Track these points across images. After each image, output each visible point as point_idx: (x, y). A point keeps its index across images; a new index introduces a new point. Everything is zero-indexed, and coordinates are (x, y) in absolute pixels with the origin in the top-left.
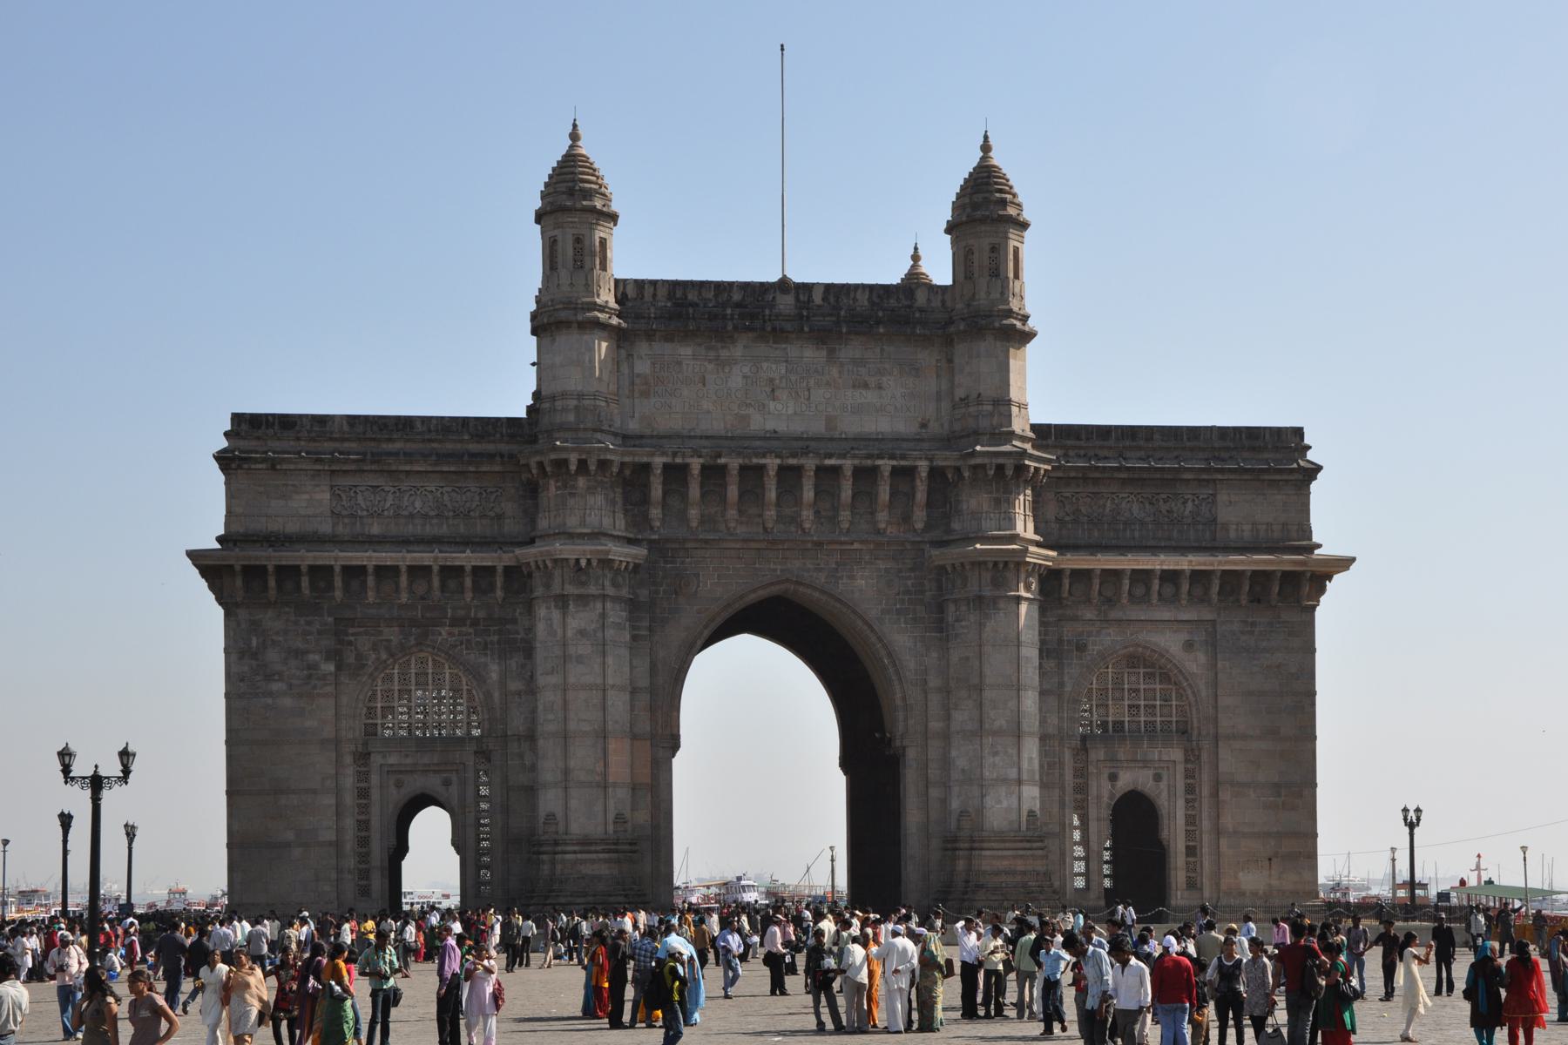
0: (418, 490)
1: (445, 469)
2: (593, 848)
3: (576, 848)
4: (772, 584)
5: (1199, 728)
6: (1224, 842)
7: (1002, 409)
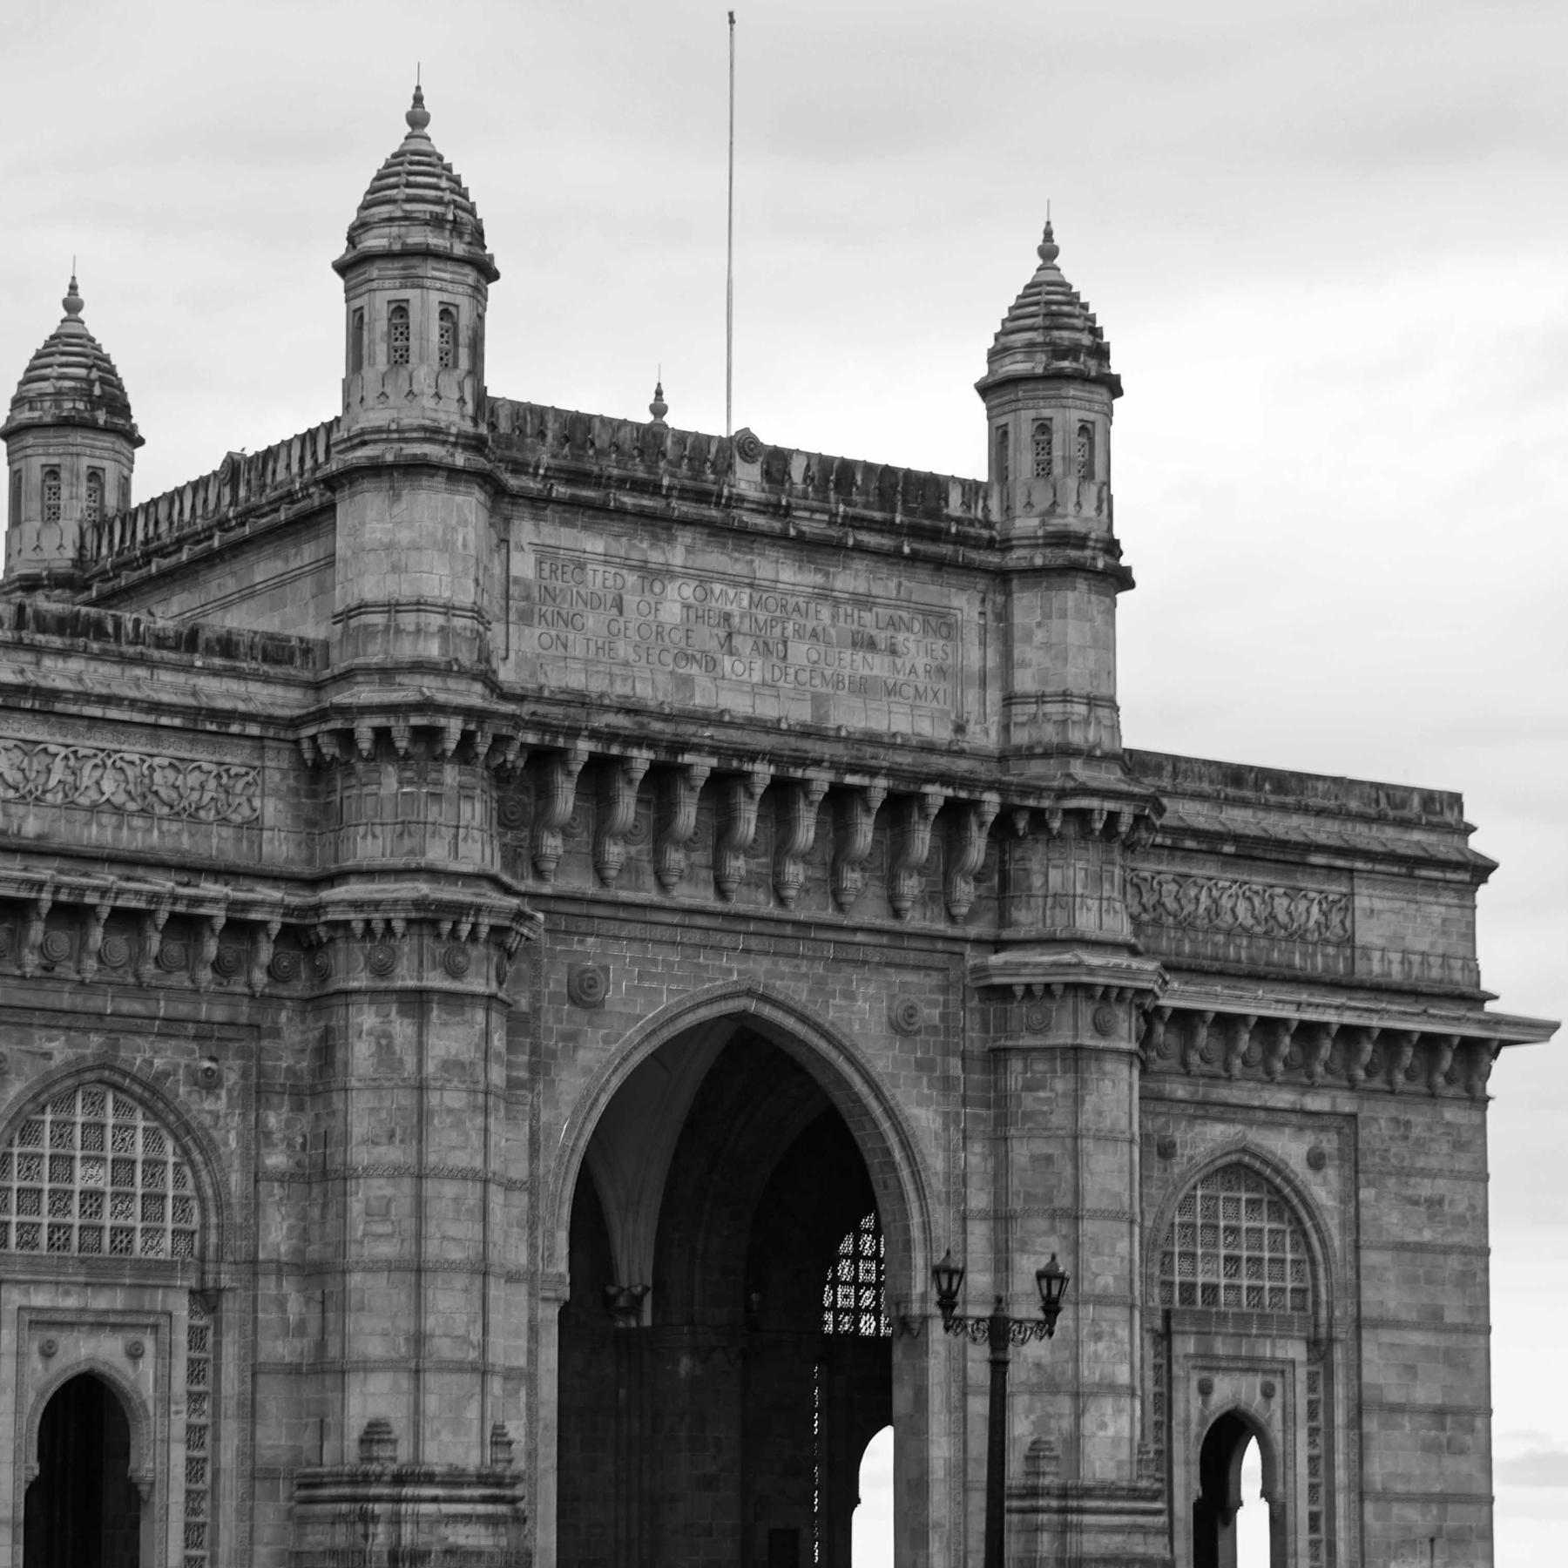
0: (109, 756)
1: (164, 721)
2: (466, 1492)
3: (439, 1492)
4: (724, 997)
5: (1330, 1306)
6: (1369, 1507)
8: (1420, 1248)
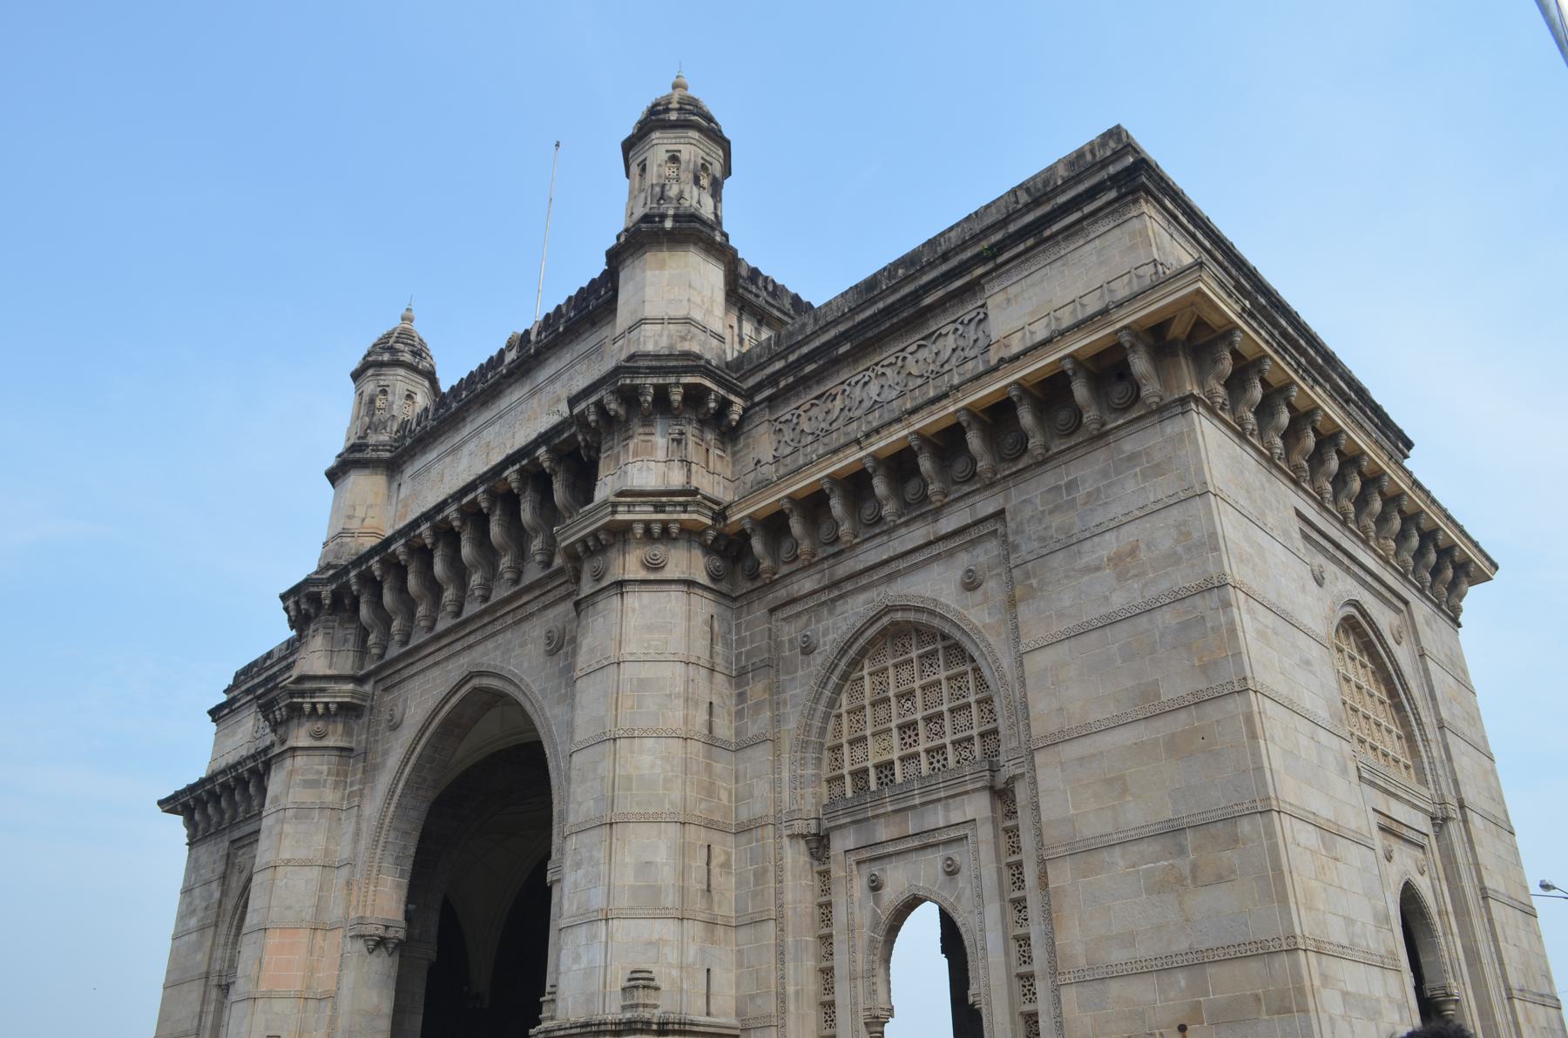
6: (1069, 996)
8: (1111, 622)
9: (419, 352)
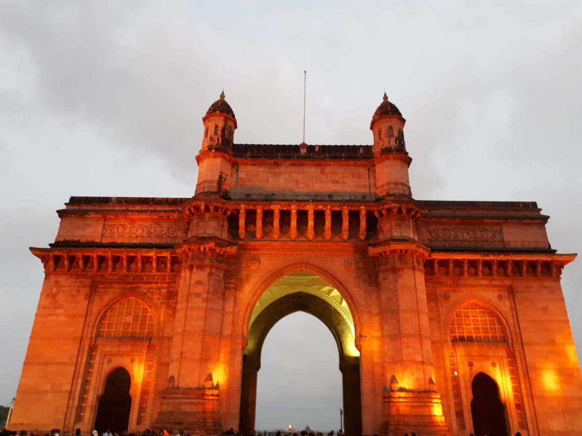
3: (181, 396)
5: (512, 339)
6: (536, 401)
7: (398, 186)
9: (233, 116)
